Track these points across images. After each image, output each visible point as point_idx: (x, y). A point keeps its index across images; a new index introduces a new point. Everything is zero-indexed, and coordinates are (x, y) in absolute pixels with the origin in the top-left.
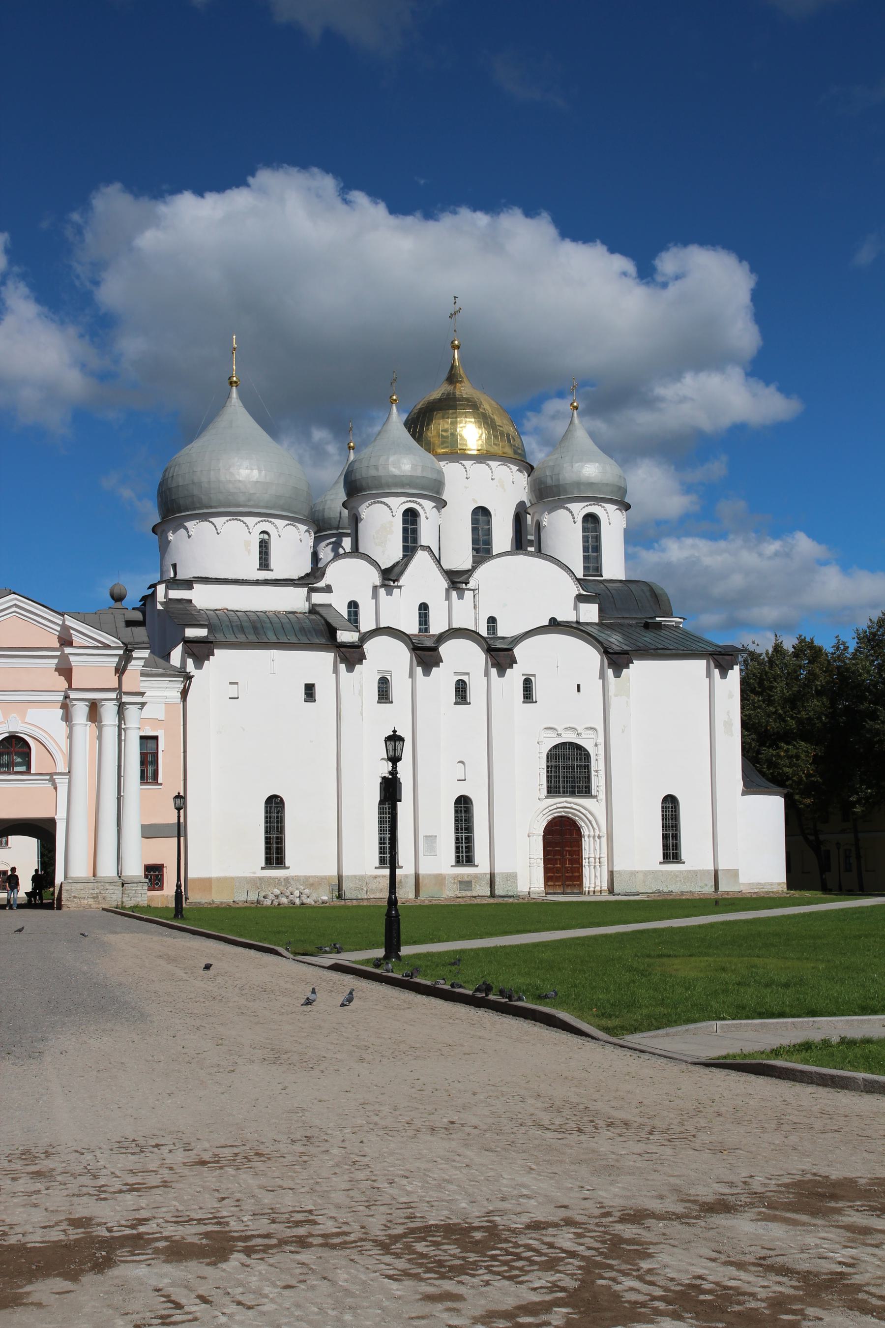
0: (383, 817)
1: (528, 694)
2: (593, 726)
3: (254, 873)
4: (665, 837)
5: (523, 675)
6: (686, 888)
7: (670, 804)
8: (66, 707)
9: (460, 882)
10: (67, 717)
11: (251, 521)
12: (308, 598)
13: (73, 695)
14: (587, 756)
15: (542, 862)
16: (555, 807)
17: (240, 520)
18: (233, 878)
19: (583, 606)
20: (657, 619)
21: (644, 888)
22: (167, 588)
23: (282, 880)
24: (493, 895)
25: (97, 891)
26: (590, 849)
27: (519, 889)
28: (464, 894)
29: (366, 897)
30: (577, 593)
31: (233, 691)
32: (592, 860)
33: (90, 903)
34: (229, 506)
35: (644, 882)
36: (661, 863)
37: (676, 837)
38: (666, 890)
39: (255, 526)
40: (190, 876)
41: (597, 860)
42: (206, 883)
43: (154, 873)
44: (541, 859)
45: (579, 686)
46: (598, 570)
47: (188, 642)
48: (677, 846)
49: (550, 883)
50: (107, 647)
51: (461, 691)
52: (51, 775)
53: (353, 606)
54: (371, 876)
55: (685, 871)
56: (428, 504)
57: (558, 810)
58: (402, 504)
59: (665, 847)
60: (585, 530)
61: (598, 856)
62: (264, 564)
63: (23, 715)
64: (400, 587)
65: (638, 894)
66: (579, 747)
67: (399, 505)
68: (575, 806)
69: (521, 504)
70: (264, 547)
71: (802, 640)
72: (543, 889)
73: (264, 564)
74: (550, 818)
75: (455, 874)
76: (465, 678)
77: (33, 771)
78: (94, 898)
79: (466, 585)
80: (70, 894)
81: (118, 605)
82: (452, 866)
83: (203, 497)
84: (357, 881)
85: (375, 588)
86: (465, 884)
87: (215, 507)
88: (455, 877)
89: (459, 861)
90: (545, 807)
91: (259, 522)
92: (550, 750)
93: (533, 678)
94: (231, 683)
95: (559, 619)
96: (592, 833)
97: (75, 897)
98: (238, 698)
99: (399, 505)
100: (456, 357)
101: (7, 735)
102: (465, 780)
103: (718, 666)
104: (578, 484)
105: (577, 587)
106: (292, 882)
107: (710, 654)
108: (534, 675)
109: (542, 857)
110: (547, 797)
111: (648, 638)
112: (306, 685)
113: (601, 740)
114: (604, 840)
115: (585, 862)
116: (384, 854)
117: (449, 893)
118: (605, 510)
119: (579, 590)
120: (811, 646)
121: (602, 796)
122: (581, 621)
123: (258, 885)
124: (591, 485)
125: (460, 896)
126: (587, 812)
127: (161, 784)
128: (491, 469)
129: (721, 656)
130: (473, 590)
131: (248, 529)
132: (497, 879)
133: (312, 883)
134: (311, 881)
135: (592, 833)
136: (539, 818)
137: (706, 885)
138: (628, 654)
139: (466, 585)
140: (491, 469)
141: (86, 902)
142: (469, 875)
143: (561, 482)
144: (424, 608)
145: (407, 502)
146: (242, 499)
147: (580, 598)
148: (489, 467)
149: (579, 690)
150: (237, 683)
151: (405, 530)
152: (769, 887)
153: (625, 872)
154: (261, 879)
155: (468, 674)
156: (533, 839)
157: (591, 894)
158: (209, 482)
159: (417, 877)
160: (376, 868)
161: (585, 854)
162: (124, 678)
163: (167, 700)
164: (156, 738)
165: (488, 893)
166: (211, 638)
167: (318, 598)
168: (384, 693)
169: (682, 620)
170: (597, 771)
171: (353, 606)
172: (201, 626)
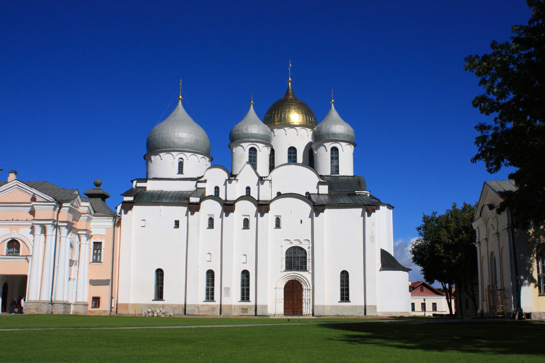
0: (209, 279)
1: (278, 225)
2: (308, 239)
3: (149, 302)
4: (342, 290)
5: (275, 216)
6: (351, 314)
7: (345, 275)
8: (32, 228)
9: (242, 309)
10: (32, 233)
11: (174, 153)
12: (196, 186)
14: (305, 253)
15: (283, 300)
16: (288, 275)
17: (170, 154)
18: (140, 304)
19: (320, 187)
20: (356, 192)
21: (329, 313)
22: (137, 182)
23: (161, 306)
24: (256, 315)
25: (37, 306)
26: (306, 295)
27: (268, 313)
28: (244, 314)
29: (198, 314)
30: (319, 181)
31: (143, 223)
32: (306, 300)
33: (34, 311)
34: (167, 148)
35: (331, 310)
36: (339, 302)
37: (348, 290)
38: (341, 314)
39: (177, 156)
40: (119, 302)
41: (308, 300)
42: (126, 306)
43: (96, 301)
44: (283, 299)
45: (301, 221)
46: (337, 172)
47: (124, 202)
48: (348, 294)
49: (287, 310)
50: (48, 201)
51: (246, 224)
52: (26, 256)
53: (217, 189)
54: (201, 305)
55: (351, 306)
56: (261, 145)
57: (290, 277)
58: (248, 145)
59: (342, 294)
60: (332, 154)
61: (309, 298)
62: (181, 171)
63: (18, 231)
64: (237, 180)
65: (323, 316)
66: (302, 249)
67: (247, 146)
68: (298, 275)
69: (310, 144)
70: (181, 165)
71: (465, 205)
72: (283, 313)
73: (181, 171)
74: (287, 280)
75: (240, 305)
76: (248, 217)
77: (21, 254)
78: (36, 309)
79: (264, 178)
80: (26, 307)
81: (97, 188)
82: (239, 301)
83: (157, 144)
84: (193, 307)
85: (226, 180)
86: (245, 310)
87: (161, 149)
88: (240, 306)
89: (243, 299)
90: (284, 275)
91: (178, 154)
92: (288, 250)
93: (280, 217)
94: (142, 220)
95: (310, 192)
96: (307, 288)
97: (28, 309)
98: (144, 227)
99: (247, 146)
100: (290, 85)
101: (10, 239)
102: (246, 263)
103: (367, 211)
104: (328, 134)
105: (319, 178)
106: (166, 307)
107: (364, 206)
108: (280, 216)
109: (283, 298)
110: (284, 271)
111: (346, 200)
112: (176, 221)
113: (311, 245)
114: (311, 291)
115: (304, 301)
116: (208, 295)
117: (236, 313)
118: (341, 145)
119: (319, 180)
120: (469, 206)
121: (310, 271)
122: (320, 193)
123: (151, 307)
124: (334, 134)
125: (242, 314)
126: (304, 278)
127: (102, 263)
128: (297, 131)
129: (369, 206)
130: (270, 181)
131: (174, 157)
132: (258, 308)
133: (174, 307)
134: (174, 306)
135: (307, 288)
136: (281, 280)
137: (361, 313)
138: (324, 206)
139: (264, 178)
140: (297, 131)
141: (32, 311)
142: (246, 306)
143: (321, 134)
144: (248, 189)
145: (251, 144)
146: (172, 145)
147: (320, 183)
148: (296, 129)
149: (301, 222)
150: (144, 220)
151: (250, 157)
152: (395, 314)
153: (320, 306)
154: (152, 305)
155: (249, 216)
156: (278, 290)
157: (305, 315)
158: (159, 138)
159: (221, 305)
160: (204, 301)
161: (304, 298)
162: (59, 215)
163: (106, 227)
164: (101, 243)
165: (254, 314)
166: (135, 201)
167: (200, 185)
168: (211, 225)
169: (368, 192)
170: (309, 259)
171: (217, 189)
172: (130, 196)
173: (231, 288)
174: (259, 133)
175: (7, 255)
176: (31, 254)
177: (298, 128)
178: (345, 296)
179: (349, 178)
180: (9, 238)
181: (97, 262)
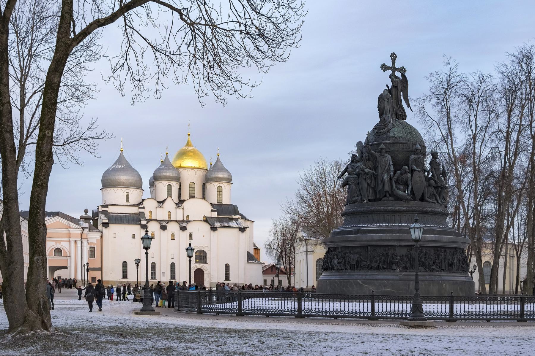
7: (227, 267)
11: (124, 189)
13: (71, 239)
14: (205, 253)
19: (213, 213)
26: (206, 277)
48: (229, 277)
53: (151, 212)
62: (127, 200)
66: (204, 251)
67: (166, 183)
70: (127, 196)
73: (127, 200)
85: (156, 207)
115: (205, 280)
155: (175, 232)
171: (151, 212)
173: (166, 273)
174: (173, 175)
175: (55, 256)
176: (68, 255)
177: (196, 170)
178: (227, 277)
179: (229, 206)
180: (56, 247)
181: (92, 258)
